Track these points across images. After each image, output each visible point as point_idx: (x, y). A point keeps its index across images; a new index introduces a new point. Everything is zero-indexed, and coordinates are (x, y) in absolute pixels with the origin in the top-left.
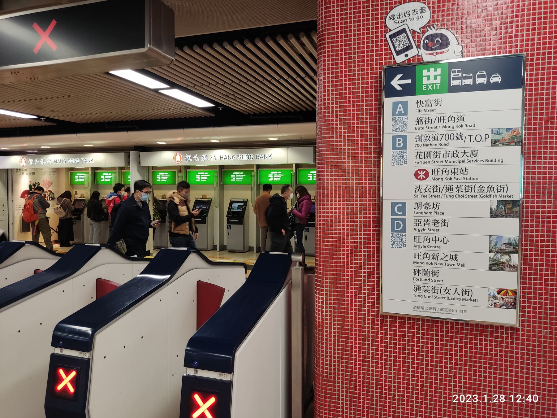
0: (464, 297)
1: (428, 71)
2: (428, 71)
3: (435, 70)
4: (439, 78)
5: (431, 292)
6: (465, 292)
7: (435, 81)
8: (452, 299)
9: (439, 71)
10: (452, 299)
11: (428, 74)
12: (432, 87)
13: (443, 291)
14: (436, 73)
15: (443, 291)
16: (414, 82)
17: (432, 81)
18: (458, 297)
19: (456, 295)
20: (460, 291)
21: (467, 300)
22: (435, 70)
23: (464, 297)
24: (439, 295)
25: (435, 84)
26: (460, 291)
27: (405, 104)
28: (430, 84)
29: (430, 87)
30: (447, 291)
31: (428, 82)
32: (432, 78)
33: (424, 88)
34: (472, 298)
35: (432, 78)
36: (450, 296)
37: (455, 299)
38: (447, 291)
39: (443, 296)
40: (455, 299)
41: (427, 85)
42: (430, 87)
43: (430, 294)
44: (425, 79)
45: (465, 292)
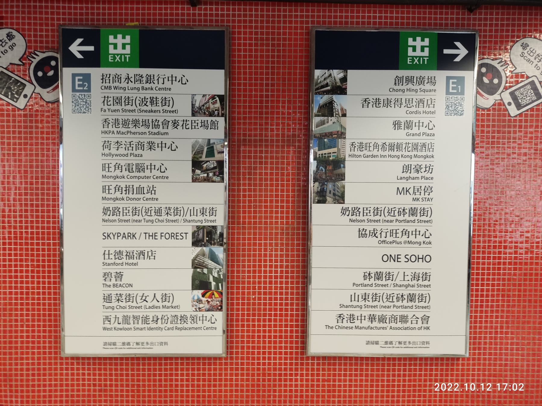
0: (164, 304)
1: (115, 37)
2: (115, 37)
3: (124, 38)
5: (124, 301)
6: (165, 297)
7: (124, 52)
8: (150, 307)
10: (150, 307)
11: (114, 41)
12: (121, 58)
13: (139, 299)
15: (139, 299)
18: (157, 304)
19: (155, 303)
20: (159, 297)
21: (168, 307)
22: (124, 38)
23: (164, 304)
24: (134, 304)
25: (124, 55)
26: (159, 297)
27: (87, 78)
28: (118, 55)
29: (118, 58)
30: (144, 298)
31: (115, 52)
33: (110, 59)
34: (174, 305)
35: (120, 46)
36: (148, 304)
37: (153, 307)
38: (144, 298)
39: (139, 305)
40: (153, 307)
41: (114, 55)
42: (118, 58)
43: (123, 304)
44: (111, 47)
45: (165, 297)
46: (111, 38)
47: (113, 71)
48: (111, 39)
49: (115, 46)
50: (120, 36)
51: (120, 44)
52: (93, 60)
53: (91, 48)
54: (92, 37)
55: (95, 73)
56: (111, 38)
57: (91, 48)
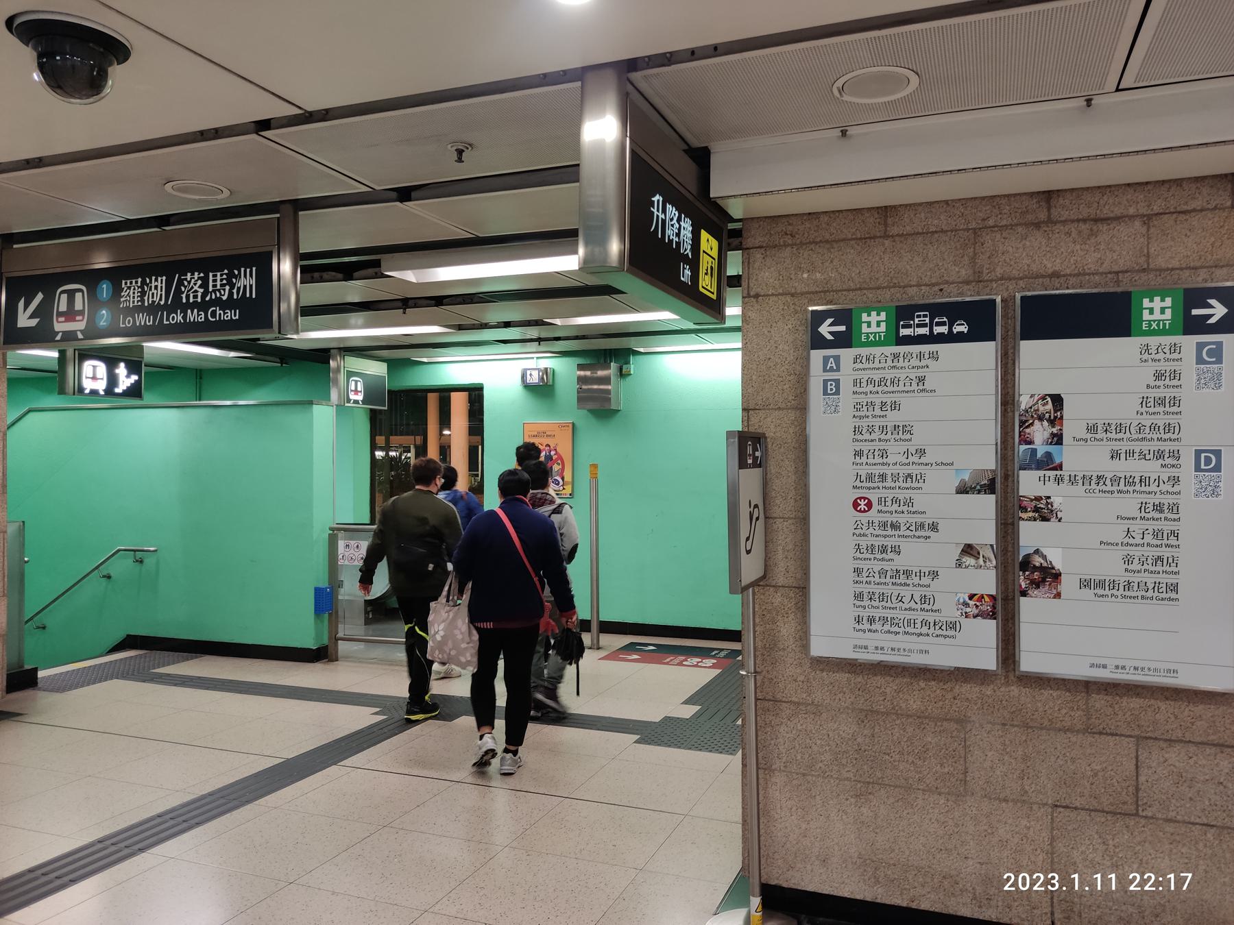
1: (869, 315)
2: (869, 315)
3: (878, 315)
4: (883, 325)
7: (879, 330)
9: (883, 314)
11: (869, 319)
14: (879, 318)
16: (849, 328)
17: (874, 329)
29: (871, 337)
32: (874, 324)
35: (874, 324)
42: (871, 337)
44: (864, 326)
46: (864, 316)
47: (864, 351)
48: (864, 317)
49: (869, 326)
50: (874, 313)
51: (874, 323)
52: (844, 341)
53: (843, 328)
54: (844, 317)
55: (846, 354)
56: (864, 317)
57: (843, 328)
